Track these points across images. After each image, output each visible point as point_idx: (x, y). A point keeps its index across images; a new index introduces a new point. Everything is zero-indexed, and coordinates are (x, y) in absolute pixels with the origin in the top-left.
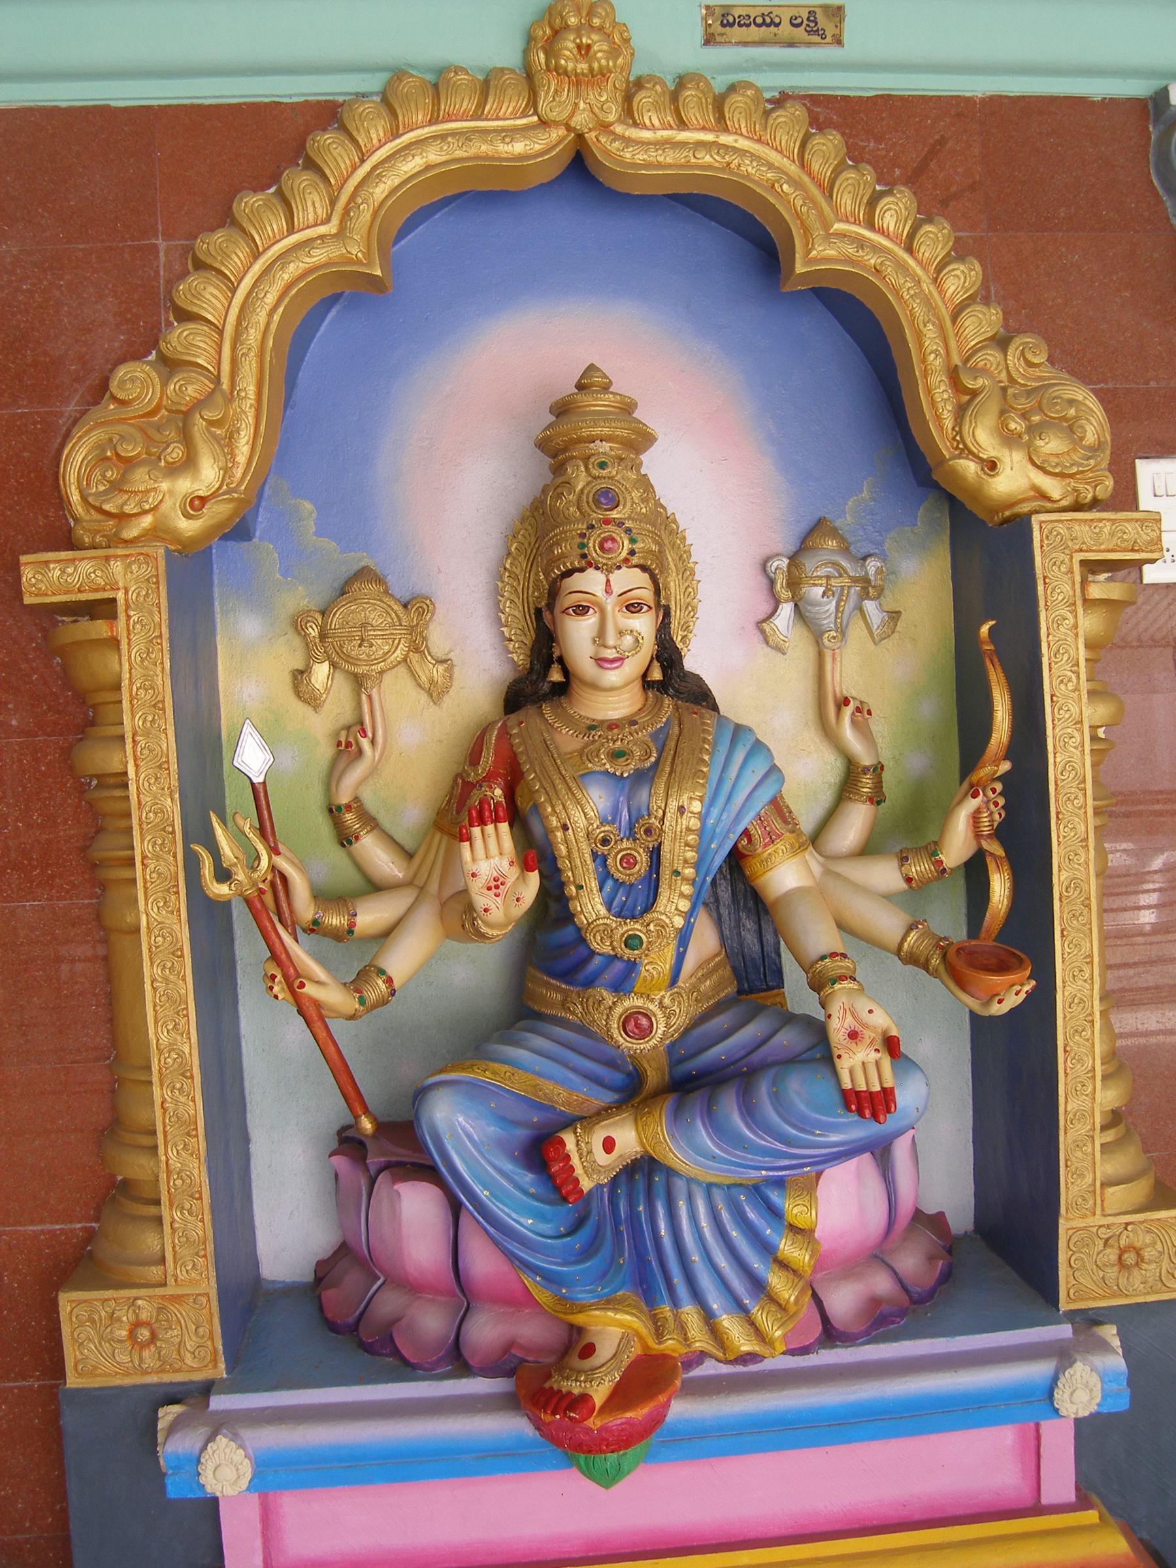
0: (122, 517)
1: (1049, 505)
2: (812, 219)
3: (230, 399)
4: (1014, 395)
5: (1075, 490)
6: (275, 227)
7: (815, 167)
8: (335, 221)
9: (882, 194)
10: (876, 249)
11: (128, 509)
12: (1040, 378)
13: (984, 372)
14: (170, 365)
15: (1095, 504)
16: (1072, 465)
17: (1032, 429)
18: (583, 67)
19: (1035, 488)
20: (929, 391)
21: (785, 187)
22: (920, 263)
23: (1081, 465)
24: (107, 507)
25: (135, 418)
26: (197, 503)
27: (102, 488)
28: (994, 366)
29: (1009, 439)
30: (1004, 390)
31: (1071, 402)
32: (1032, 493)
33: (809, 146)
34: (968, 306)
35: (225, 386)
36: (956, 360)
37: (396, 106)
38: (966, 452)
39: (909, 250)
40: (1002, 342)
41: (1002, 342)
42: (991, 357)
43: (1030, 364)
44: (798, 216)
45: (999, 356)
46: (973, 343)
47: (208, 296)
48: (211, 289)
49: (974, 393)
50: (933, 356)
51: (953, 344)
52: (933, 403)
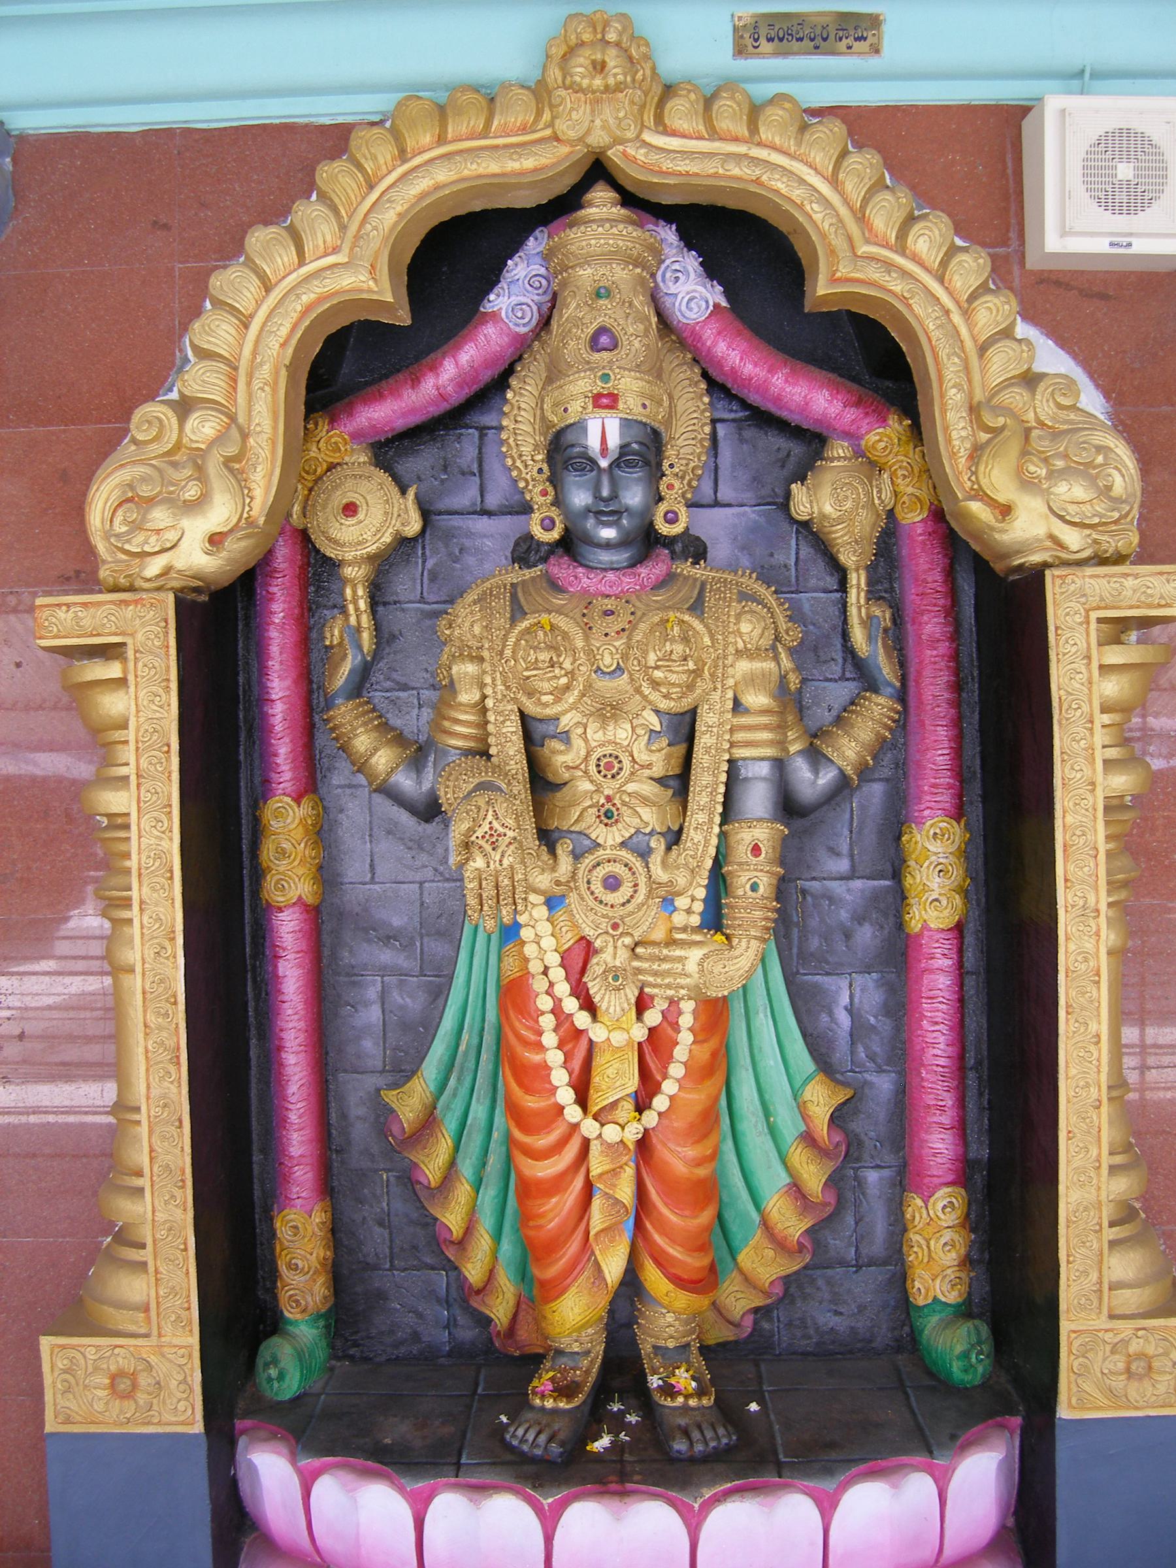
0: (144, 555)
2: (839, 243)
3: (245, 436)
4: (1040, 437)
5: (1095, 541)
6: (286, 259)
8: (346, 248)
10: (905, 274)
11: (147, 549)
12: (1071, 422)
16: (1094, 515)
17: (1051, 474)
18: (598, 82)
19: (1052, 538)
20: (946, 428)
24: (127, 547)
25: (155, 458)
26: (215, 540)
27: (124, 529)
28: (1021, 405)
29: (1027, 484)
30: (1028, 431)
31: (1099, 449)
32: (1049, 544)
34: (996, 341)
35: (241, 420)
36: (979, 396)
38: (980, 495)
42: (1016, 397)
43: (1060, 407)
44: (823, 236)
45: (1026, 395)
47: (223, 333)
48: (225, 326)
49: (996, 431)
50: (954, 391)
51: (977, 377)
52: (949, 441)
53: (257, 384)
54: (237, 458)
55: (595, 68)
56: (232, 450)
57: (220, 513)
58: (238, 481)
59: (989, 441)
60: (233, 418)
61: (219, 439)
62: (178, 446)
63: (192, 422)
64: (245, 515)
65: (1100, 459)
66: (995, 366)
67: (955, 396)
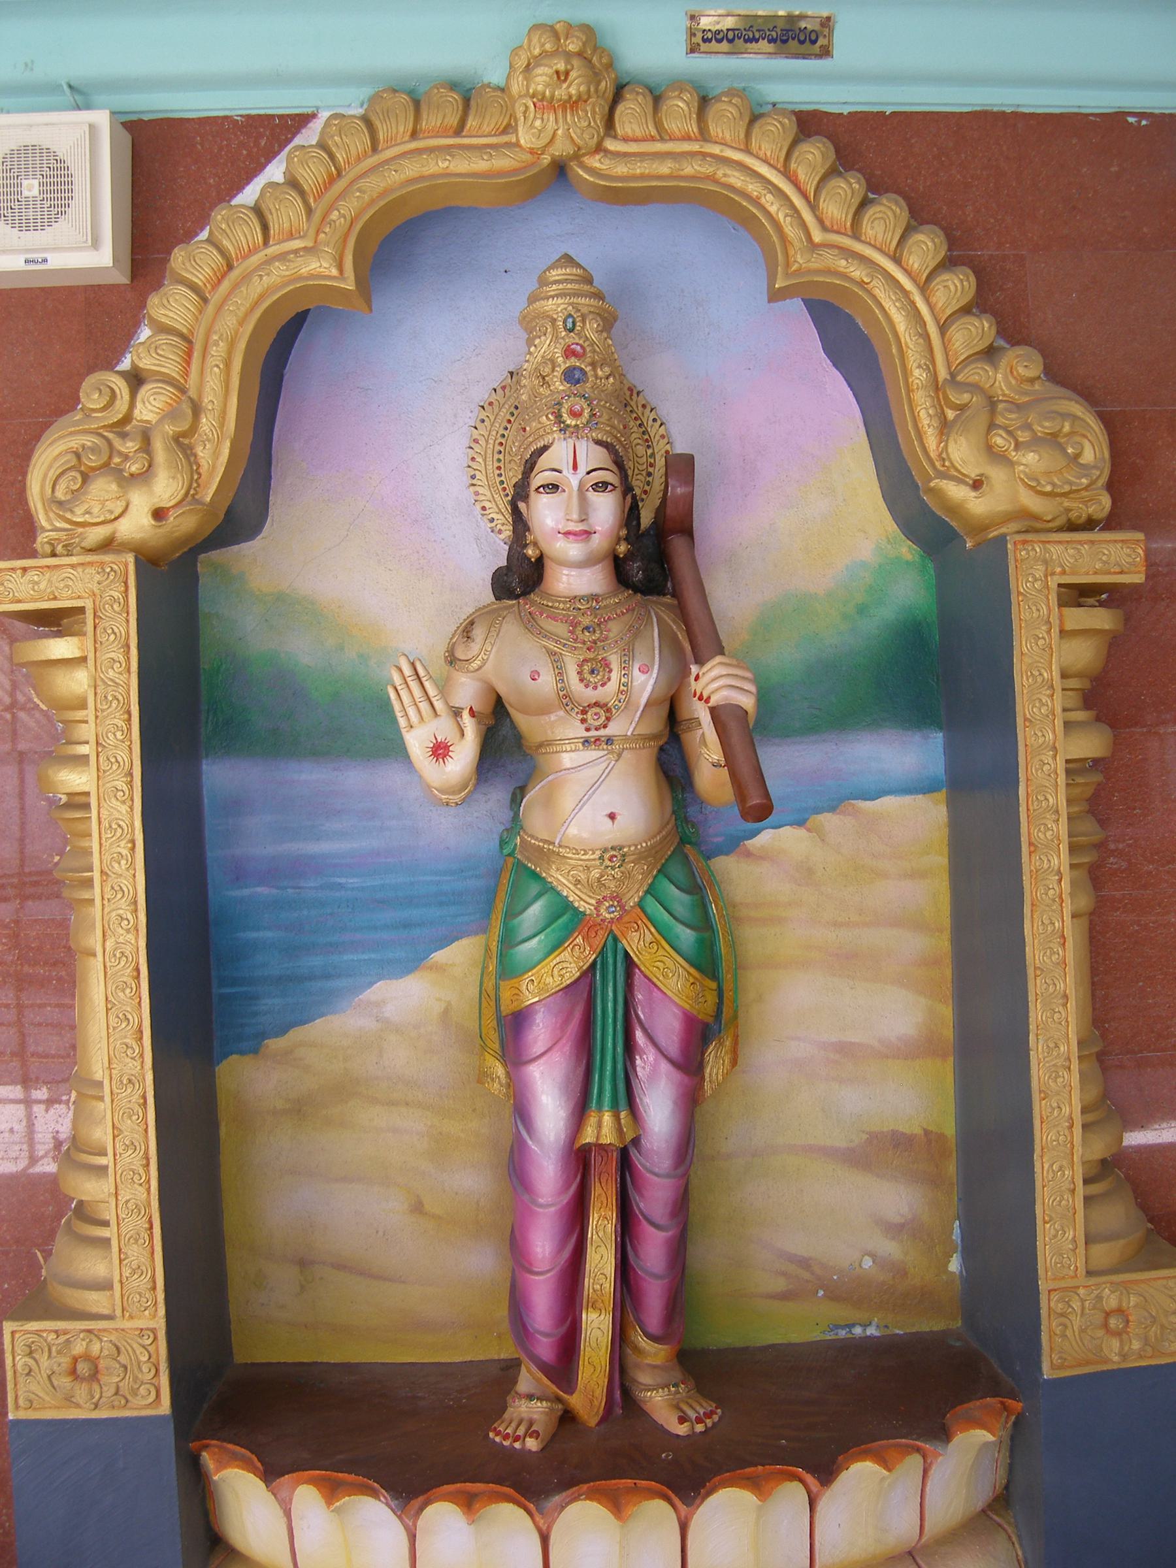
1: (1038, 525)
7: (802, 177)
8: (312, 232)
9: (872, 201)
13: (975, 388)
14: (136, 379)
15: (1089, 525)
21: (769, 197)
22: (908, 273)
23: (1071, 483)
24: (68, 515)
31: (1065, 416)
33: (796, 154)
35: (192, 393)
37: (377, 123)
39: (897, 260)
40: (990, 354)
41: (990, 354)
46: (962, 358)
49: (962, 408)
53: (210, 361)
54: (184, 434)
55: (559, 77)
56: (185, 426)
57: (166, 487)
58: (187, 457)
59: (957, 417)
60: (183, 391)
61: (171, 415)
62: (127, 418)
63: (145, 391)
64: (192, 492)
65: (1067, 428)
66: (958, 344)
67: (919, 376)
